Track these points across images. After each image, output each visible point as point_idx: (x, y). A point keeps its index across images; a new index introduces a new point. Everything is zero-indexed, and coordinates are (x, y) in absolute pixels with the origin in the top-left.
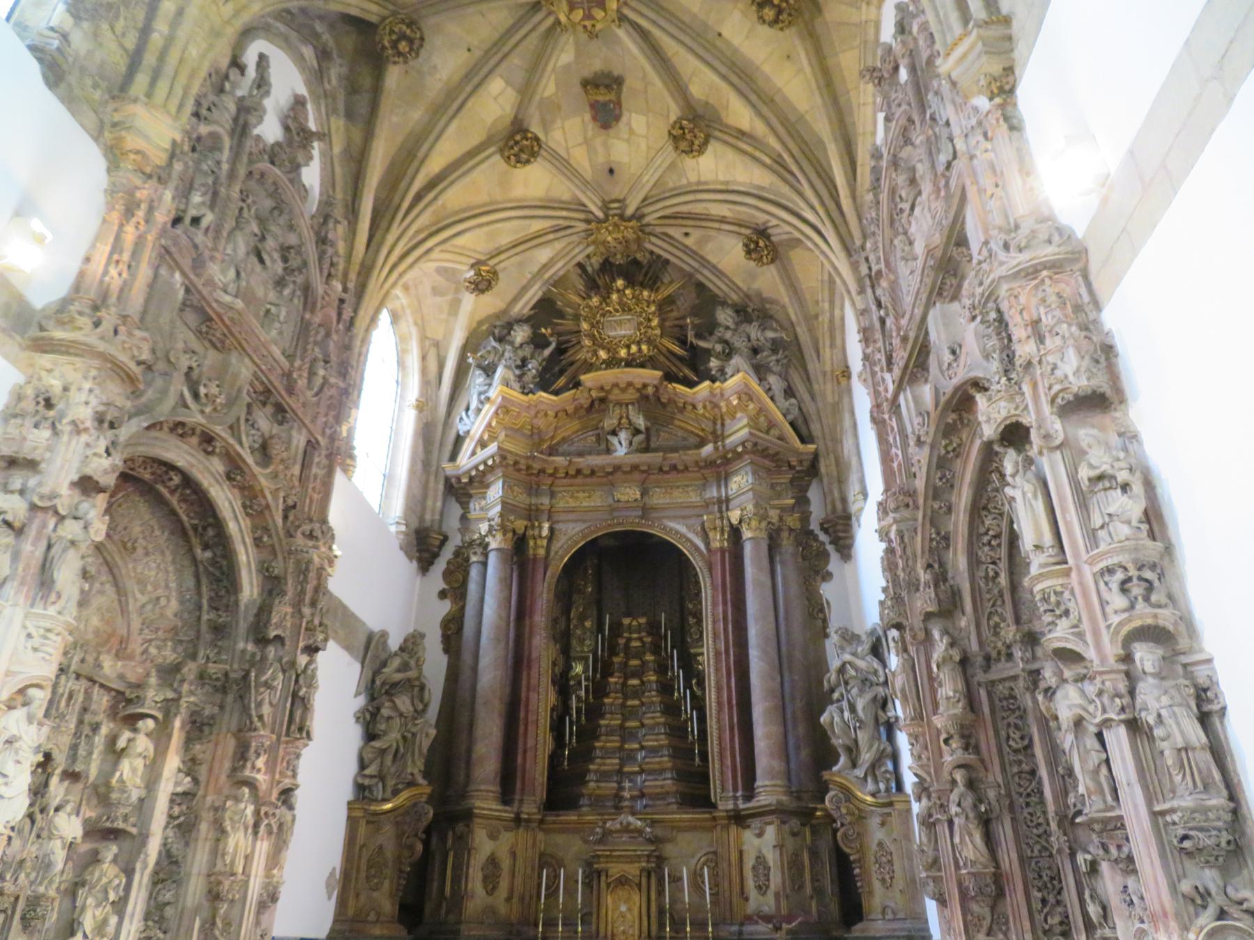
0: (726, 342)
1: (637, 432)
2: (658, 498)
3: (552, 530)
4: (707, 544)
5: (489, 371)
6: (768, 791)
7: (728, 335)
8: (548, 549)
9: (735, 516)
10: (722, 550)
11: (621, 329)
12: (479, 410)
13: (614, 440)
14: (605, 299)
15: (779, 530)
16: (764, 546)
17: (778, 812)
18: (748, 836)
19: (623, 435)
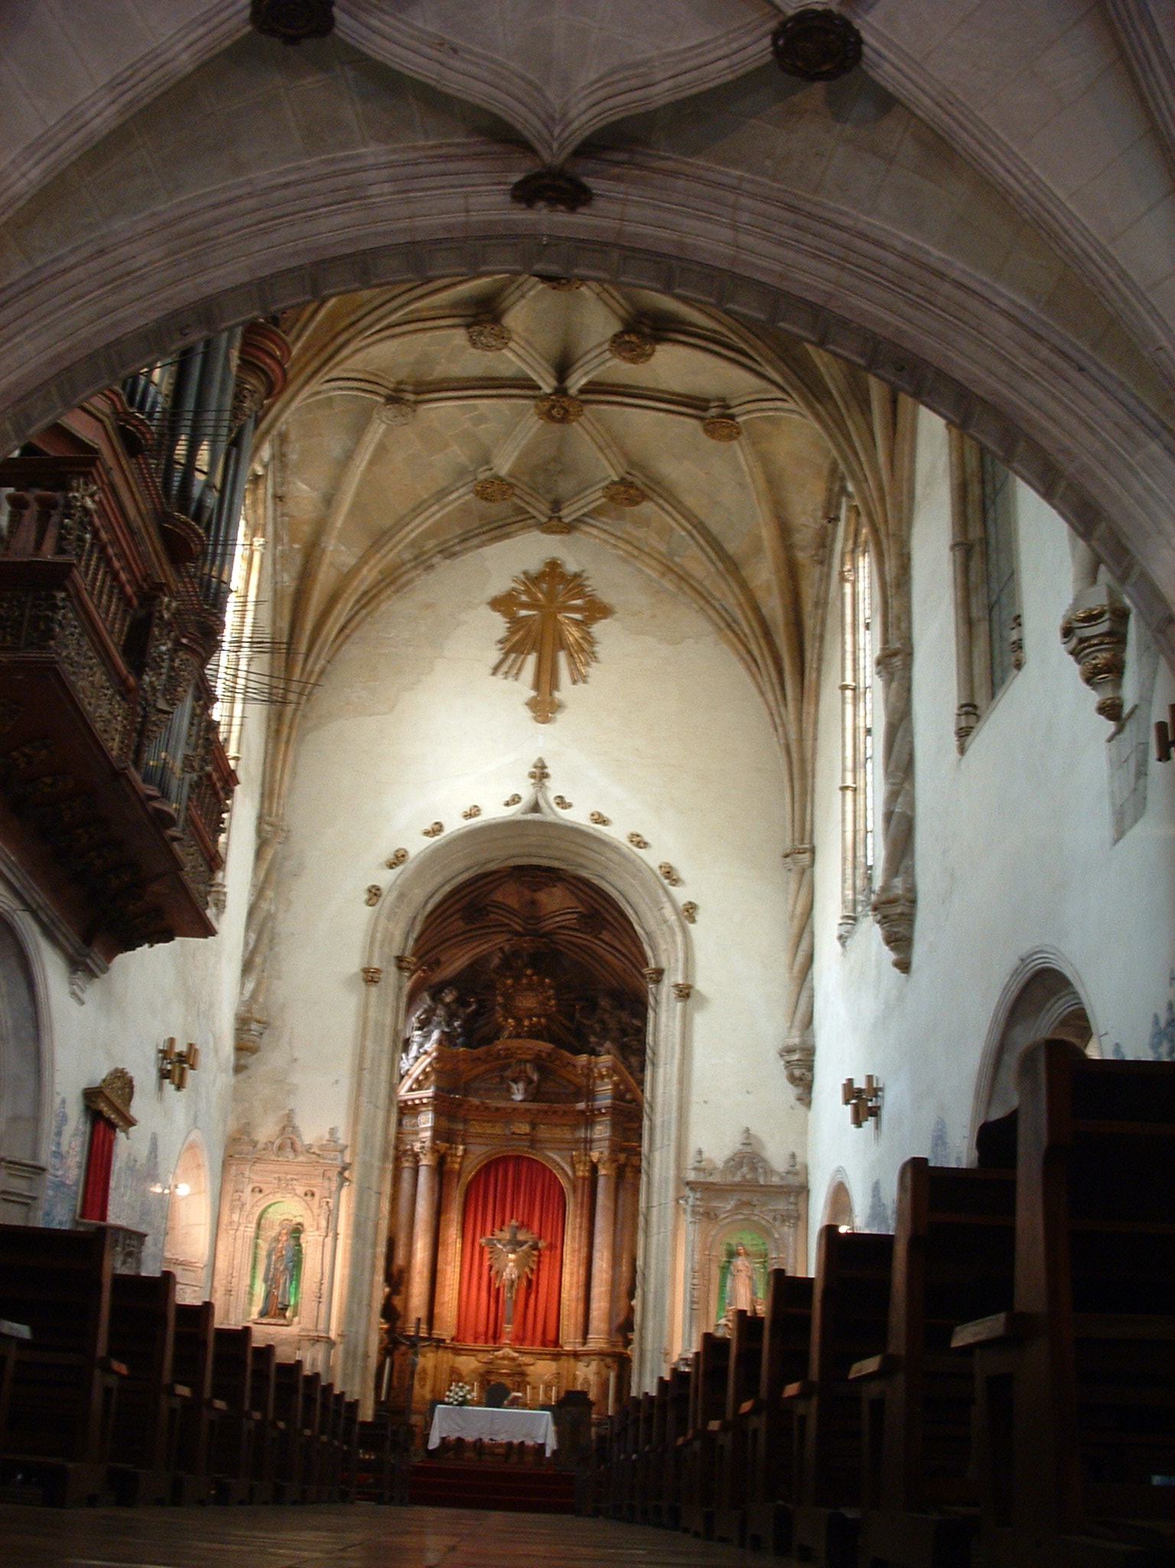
0: (602, 1021)
1: (530, 1081)
2: (543, 1132)
3: (465, 1150)
4: (574, 1172)
5: (423, 1025)
6: (598, 1340)
7: (606, 1016)
8: (461, 1163)
9: (595, 1155)
10: (584, 1178)
11: (527, 1002)
12: (417, 1058)
13: (514, 1086)
14: (517, 979)
15: (625, 1165)
16: (613, 1180)
17: (601, 1354)
18: (581, 1365)
19: (521, 1086)
